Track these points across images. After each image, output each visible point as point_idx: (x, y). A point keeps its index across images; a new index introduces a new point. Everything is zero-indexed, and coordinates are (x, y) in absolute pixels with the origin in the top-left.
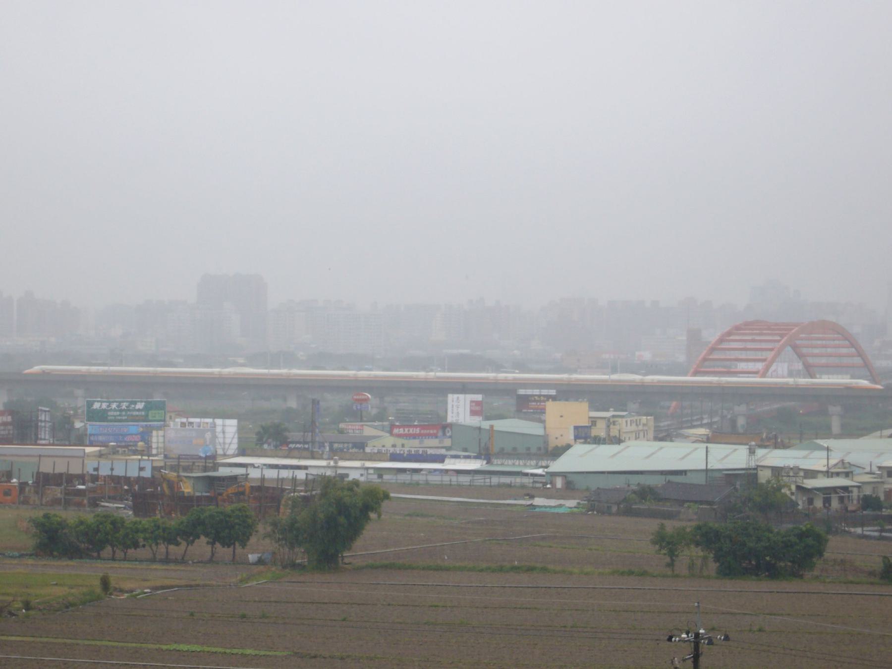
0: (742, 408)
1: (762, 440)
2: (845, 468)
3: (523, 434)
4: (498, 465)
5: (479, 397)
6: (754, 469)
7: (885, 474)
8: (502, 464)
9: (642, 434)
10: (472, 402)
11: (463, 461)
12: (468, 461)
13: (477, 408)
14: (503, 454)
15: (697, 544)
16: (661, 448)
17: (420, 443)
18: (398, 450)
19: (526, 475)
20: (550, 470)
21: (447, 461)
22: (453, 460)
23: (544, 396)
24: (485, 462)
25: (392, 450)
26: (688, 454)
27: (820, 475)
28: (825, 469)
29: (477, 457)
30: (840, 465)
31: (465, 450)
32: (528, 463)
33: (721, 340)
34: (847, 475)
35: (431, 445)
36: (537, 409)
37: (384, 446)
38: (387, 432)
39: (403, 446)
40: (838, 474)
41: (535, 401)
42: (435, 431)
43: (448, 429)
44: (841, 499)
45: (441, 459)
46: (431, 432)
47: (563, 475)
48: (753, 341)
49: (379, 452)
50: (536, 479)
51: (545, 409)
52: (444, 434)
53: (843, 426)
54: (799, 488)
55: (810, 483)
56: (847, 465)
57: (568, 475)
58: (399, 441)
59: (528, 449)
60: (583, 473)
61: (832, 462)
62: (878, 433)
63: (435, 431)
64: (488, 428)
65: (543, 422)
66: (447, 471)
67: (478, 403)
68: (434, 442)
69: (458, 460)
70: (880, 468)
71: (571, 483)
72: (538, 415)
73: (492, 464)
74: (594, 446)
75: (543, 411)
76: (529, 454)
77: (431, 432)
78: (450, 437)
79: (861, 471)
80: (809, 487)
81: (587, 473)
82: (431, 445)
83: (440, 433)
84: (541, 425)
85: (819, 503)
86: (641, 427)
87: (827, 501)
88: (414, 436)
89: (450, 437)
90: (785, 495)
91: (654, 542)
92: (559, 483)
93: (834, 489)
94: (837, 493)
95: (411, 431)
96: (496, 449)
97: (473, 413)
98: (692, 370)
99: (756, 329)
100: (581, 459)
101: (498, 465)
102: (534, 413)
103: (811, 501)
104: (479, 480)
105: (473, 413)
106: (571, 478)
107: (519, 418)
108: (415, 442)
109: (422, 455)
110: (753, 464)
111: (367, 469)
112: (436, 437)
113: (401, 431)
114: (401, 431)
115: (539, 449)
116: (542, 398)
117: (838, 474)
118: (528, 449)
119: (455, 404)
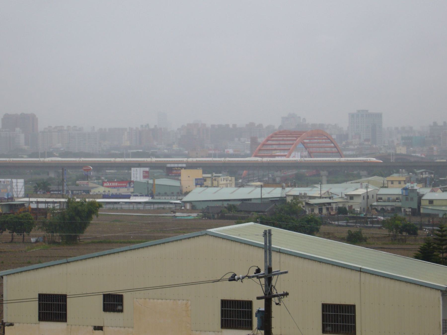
0: (278, 173)
3: (170, 186)
5: (147, 169)
7: (349, 198)
8: (159, 199)
9: (229, 185)
10: (144, 171)
11: (140, 197)
13: (146, 175)
19: (172, 203)
21: (131, 198)
22: (134, 197)
23: (180, 167)
24: (151, 198)
25: (103, 193)
28: (319, 195)
29: (147, 196)
30: (327, 194)
33: (268, 140)
34: (330, 198)
35: (123, 191)
42: (125, 184)
43: (132, 183)
44: (328, 209)
45: (128, 197)
46: (123, 185)
48: (283, 140)
51: (180, 174)
52: (130, 186)
54: (307, 204)
55: (312, 201)
56: (330, 194)
57: (192, 202)
58: (107, 190)
60: (200, 201)
61: (323, 192)
63: (125, 184)
65: (180, 180)
67: (147, 172)
69: (137, 197)
70: (346, 195)
72: (177, 176)
75: (179, 175)
77: (123, 185)
78: (133, 187)
80: (312, 203)
83: (128, 185)
85: (316, 211)
86: (228, 182)
87: (321, 210)
88: (114, 187)
89: (133, 187)
90: (300, 207)
92: (188, 206)
93: (324, 204)
94: (325, 206)
97: (145, 177)
98: (253, 155)
100: (198, 194)
102: (175, 176)
103: (313, 210)
106: (194, 204)
112: (126, 187)
113: (108, 184)
116: (179, 168)
117: (326, 198)
119: (135, 173)
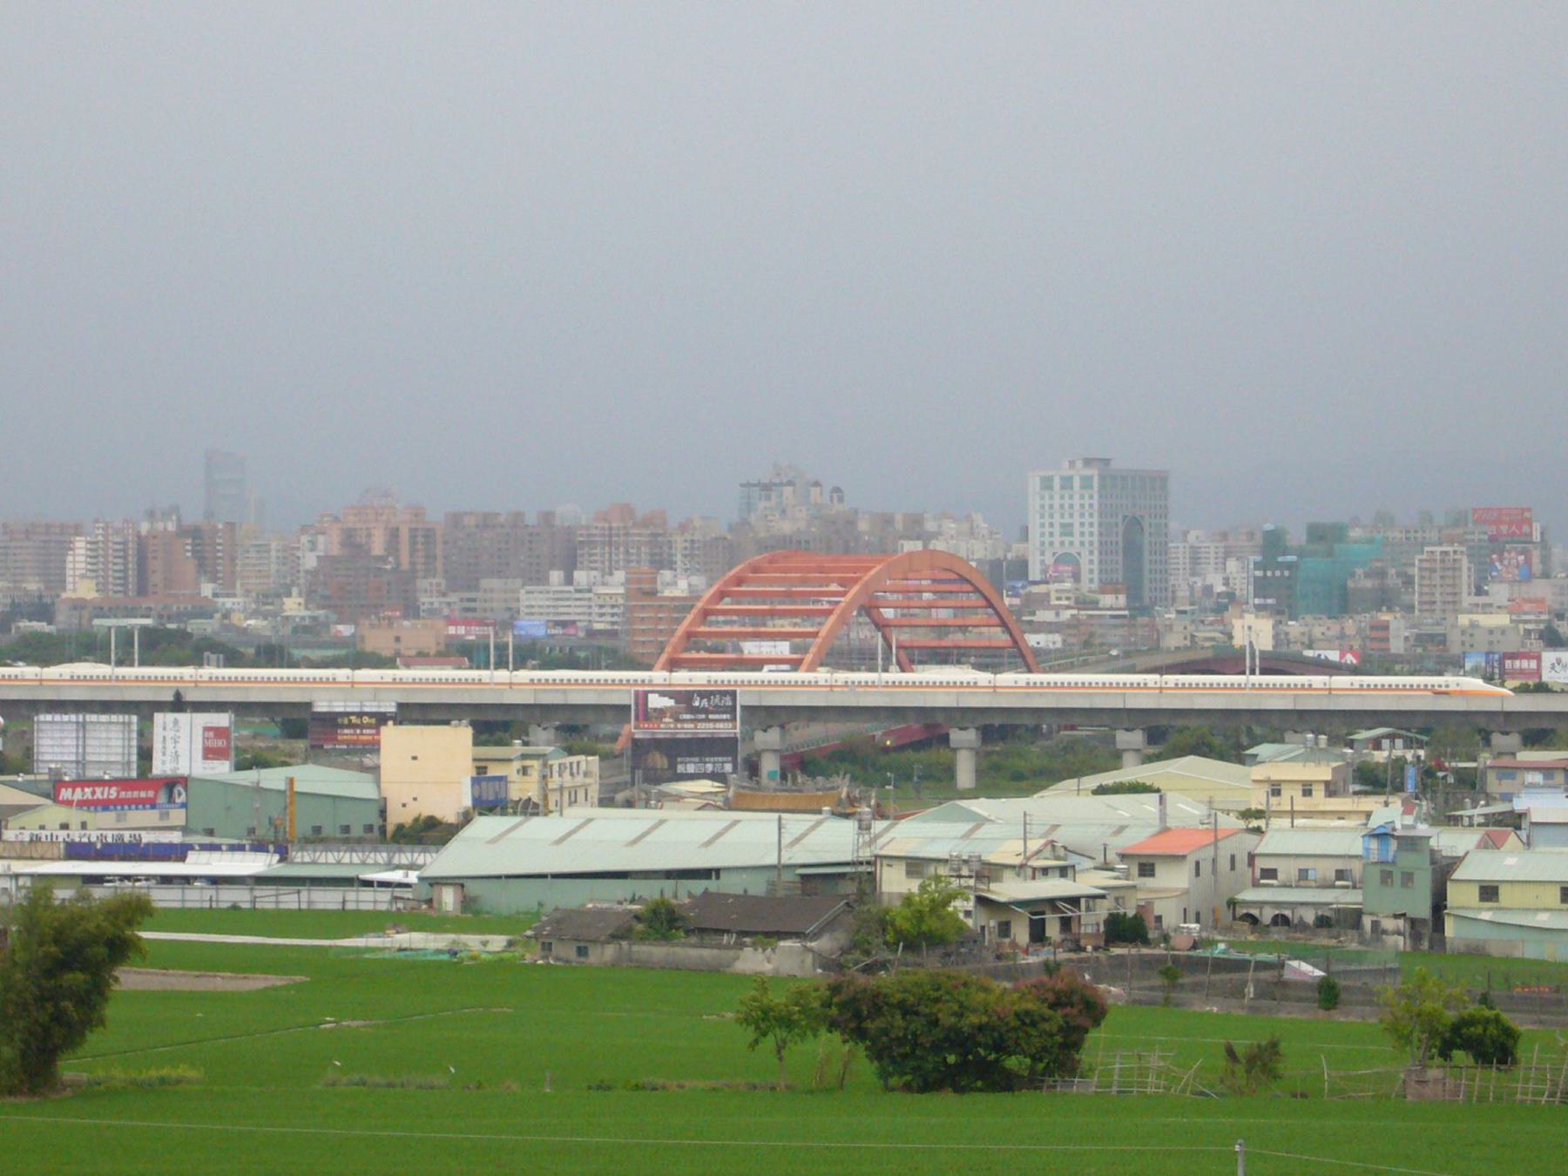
0: (772, 738)
1: (840, 802)
2: (1057, 858)
3: (335, 797)
4: (305, 862)
5: (223, 720)
6: (868, 863)
7: (1135, 870)
8: (314, 863)
9: (581, 795)
10: (206, 729)
11: (228, 855)
12: (238, 855)
13: (220, 743)
14: (317, 839)
15: (833, 1025)
16: (662, 822)
17: (118, 820)
18: (76, 835)
19: (368, 884)
20: (432, 871)
21: (192, 856)
22: (205, 855)
23: (370, 715)
24: (277, 857)
25: (62, 835)
26: (720, 834)
27: (1008, 874)
28: (1017, 861)
29: (259, 847)
30: (1048, 852)
31: (210, 833)
32: (372, 858)
33: (721, 595)
34: (1063, 871)
35: (143, 824)
36: (355, 743)
37: (42, 828)
38: (47, 796)
39: (84, 826)
40: (1045, 871)
41: (351, 726)
42: (151, 794)
43: (179, 788)
44: (1066, 924)
45: (178, 853)
46: (143, 794)
47: (458, 882)
48: (789, 595)
49: (35, 840)
50: (399, 892)
51: (378, 743)
52: (171, 799)
53: (980, 773)
54: (982, 901)
55: (1008, 889)
56: (1062, 853)
57: (467, 883)
58: (75, 816)
59: (346, 829)
60: (499, 877)
61: (1034, 845)
62: (1071, 783)
63: (151, 794)
64: (282, 786)
65: (375, 770)
66: (187, 880)
67: (220, 732)
68: (150, 817)
69: (216, 855)
70: (1124, 857)
71: (475, 902)
72: (362, 756)
73: (292, 863)
74: (518, 819)
75: (374, 747)
76: (346, 841)
77: (143, 794)
78: (184, 805)
79: (1089, 864)
80: (1002, 899)
81: (508, 877)
82: (143, 824)
83: (162, 798)
84: (368, 776)
85: (1021, 933)
86: (579, 779)
88: (105, 805)
89: (184, 805)
90: (953, 915)
91: (746, 1020)
92: (449, 899)
93: (1052, 903)
94: (1056, 909)
95: (99, 795)
96: (303, 827)
97: (210, 753)
98: (664, 658)
99: (796, 570)
100: (486, 848)
101: (305, 862)
102: (348, 752)
103: (1005, 929)
104: (267, 899)
105: (210, 753)
106: (473, 889)
107: (315, 763)
108: (108, 818)
109: (130, 845)
110: (866, 854)
111: (17, 876)
112: (153, 807)
113: (78, 795)
114: (78, 795)
115: (369, 828)
116: (366, 720)
117: (1045, 871)
118: (346, 829)
119: (170, 734)
